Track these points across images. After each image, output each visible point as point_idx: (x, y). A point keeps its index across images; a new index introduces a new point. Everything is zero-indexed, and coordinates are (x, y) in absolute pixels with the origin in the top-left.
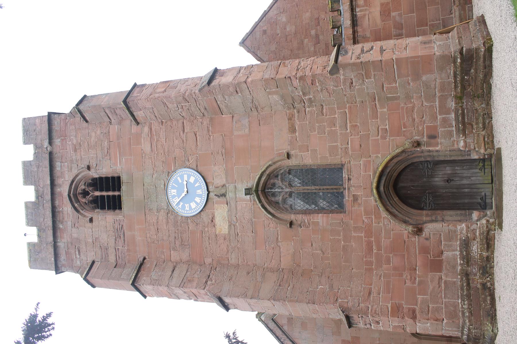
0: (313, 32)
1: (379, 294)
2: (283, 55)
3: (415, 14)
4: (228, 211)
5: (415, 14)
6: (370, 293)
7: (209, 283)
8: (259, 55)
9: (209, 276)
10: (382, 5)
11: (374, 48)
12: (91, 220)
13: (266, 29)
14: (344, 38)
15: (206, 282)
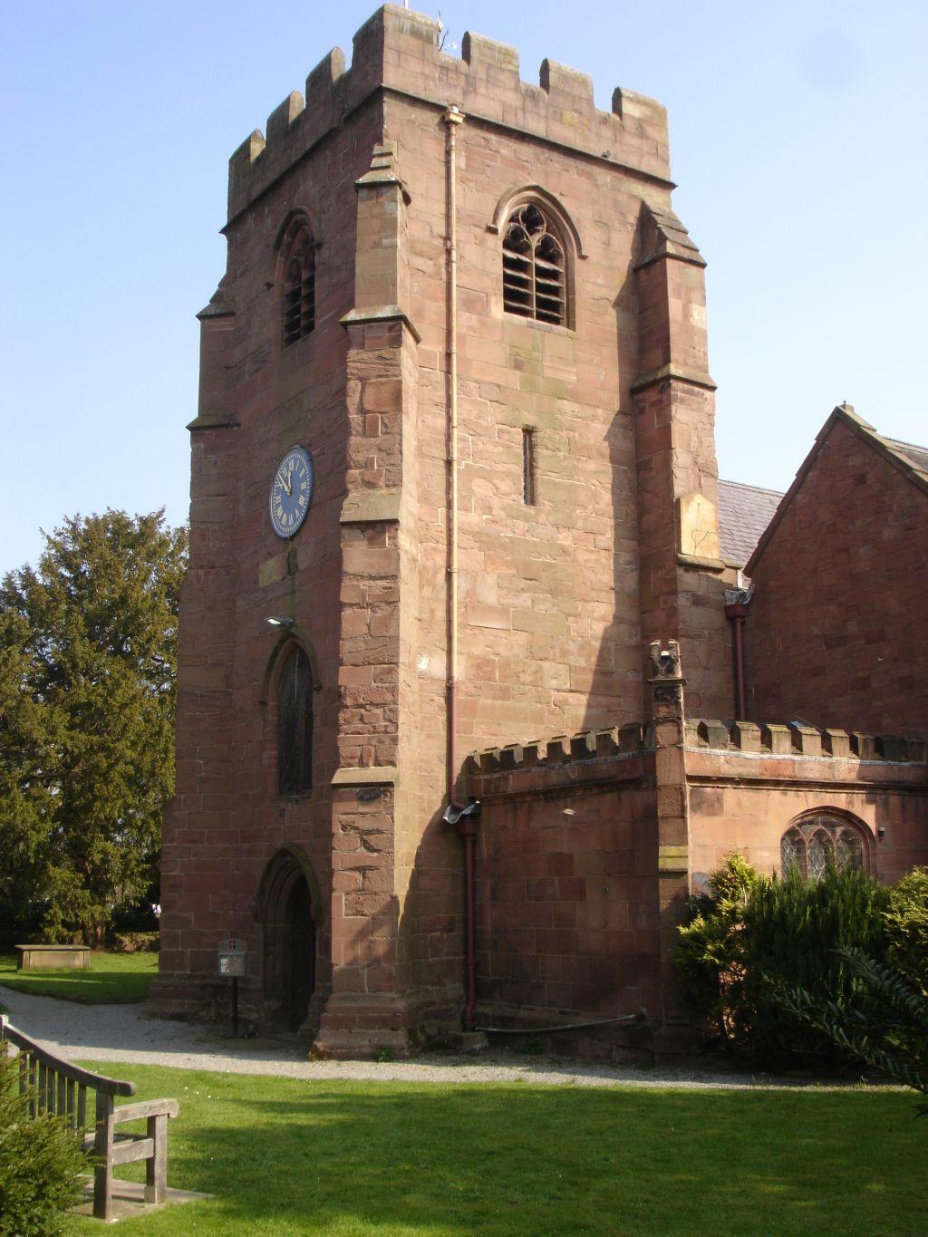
0: (852, 628)
1: (195, 855)
2: (808, 546)
3: (553, 928)
4: (277, 583)
5: (553, 928)
6: (195, 842)
7: (201, 572)
8: (810, 474)
9: (213, 567)
10: (570, 857)
11: (375, 854)
12: (269, 286)
13: (868, 482)
14: (530, 771)
15: (201, 567)
